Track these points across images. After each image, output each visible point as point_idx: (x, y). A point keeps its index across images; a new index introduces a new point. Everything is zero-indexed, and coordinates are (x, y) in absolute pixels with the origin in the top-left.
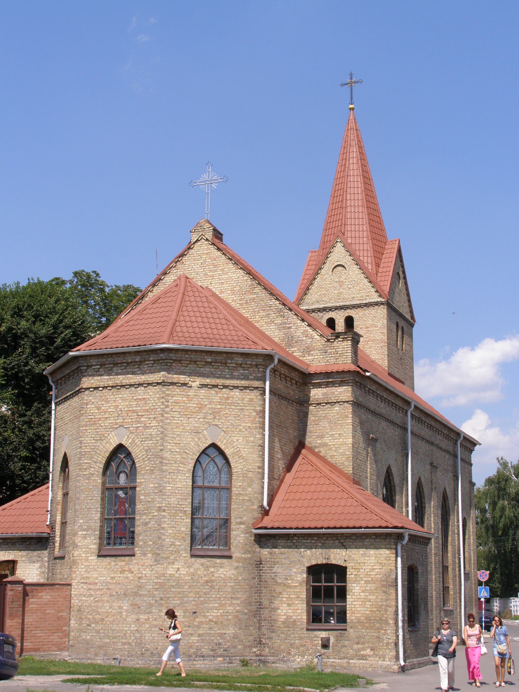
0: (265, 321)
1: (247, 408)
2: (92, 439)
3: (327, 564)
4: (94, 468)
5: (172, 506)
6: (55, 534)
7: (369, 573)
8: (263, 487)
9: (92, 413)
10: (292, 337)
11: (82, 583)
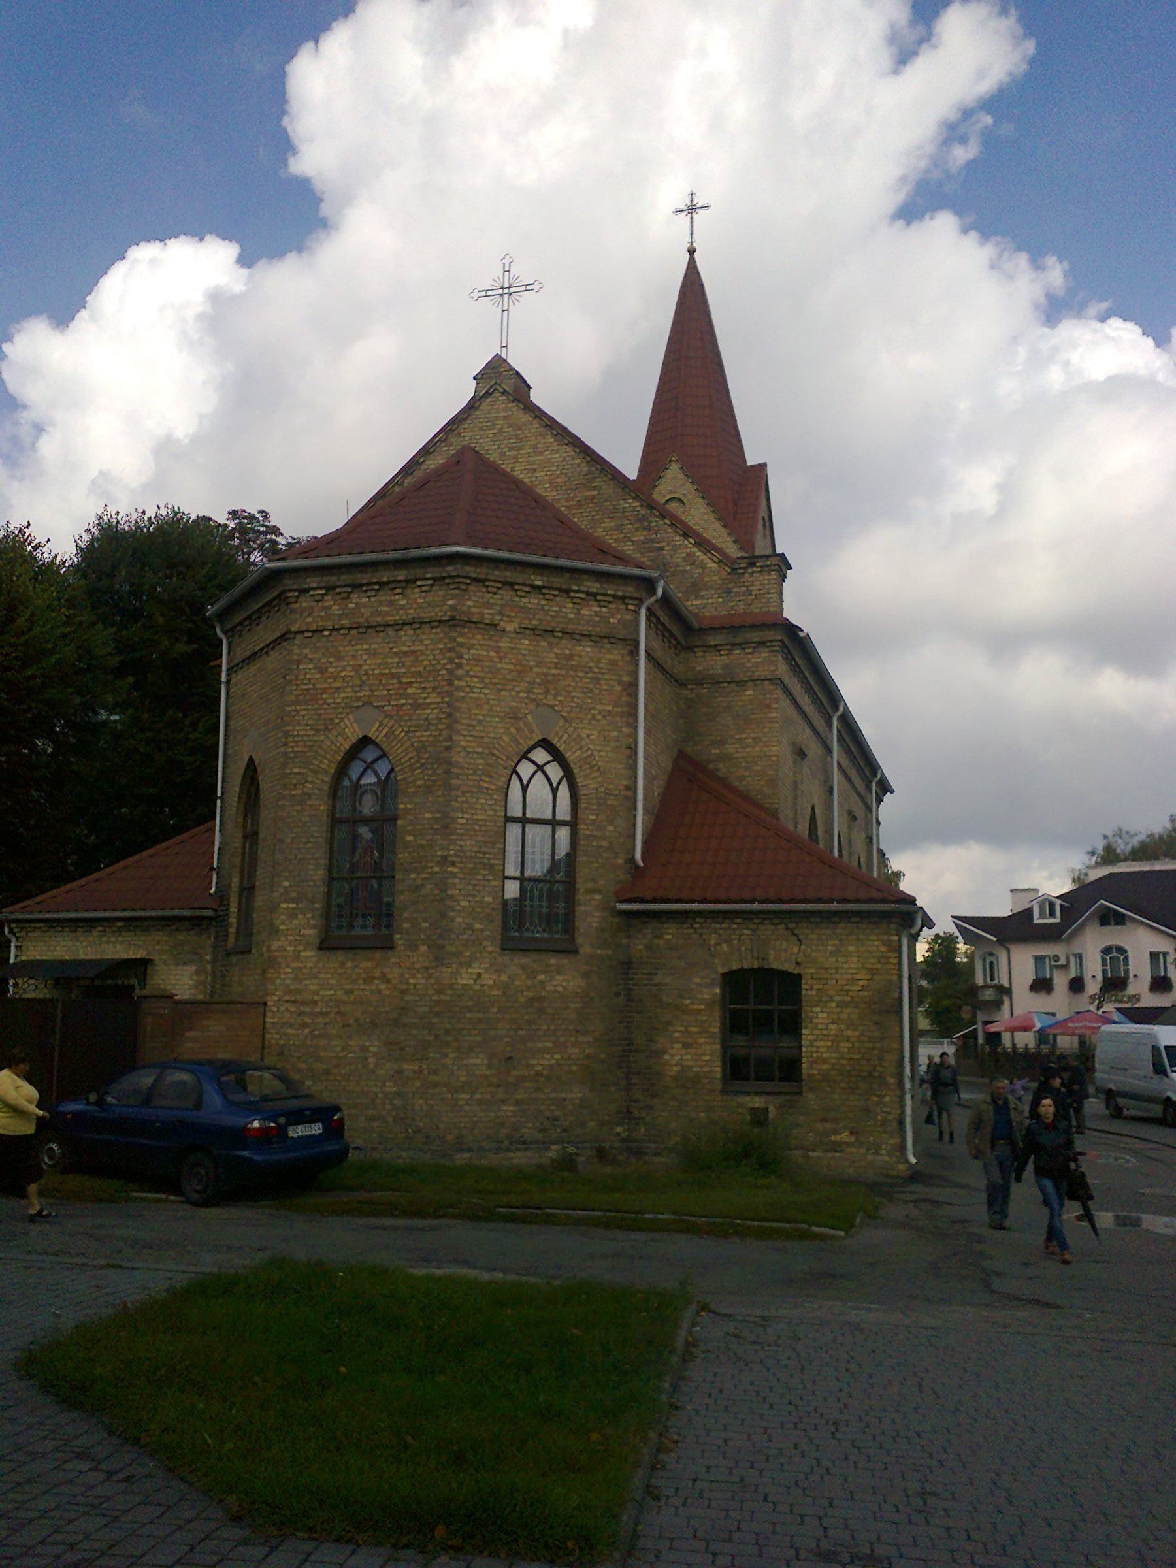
0: (614, 537)
1: (606, 676)
2: (308, 728)
4: (312, 782)
5: (468, 854)
6: (228, 910)
7: (847, 988)
8: (634, 825)
9: (310, 679)
10: (665, 565)
11: (287, 1001)
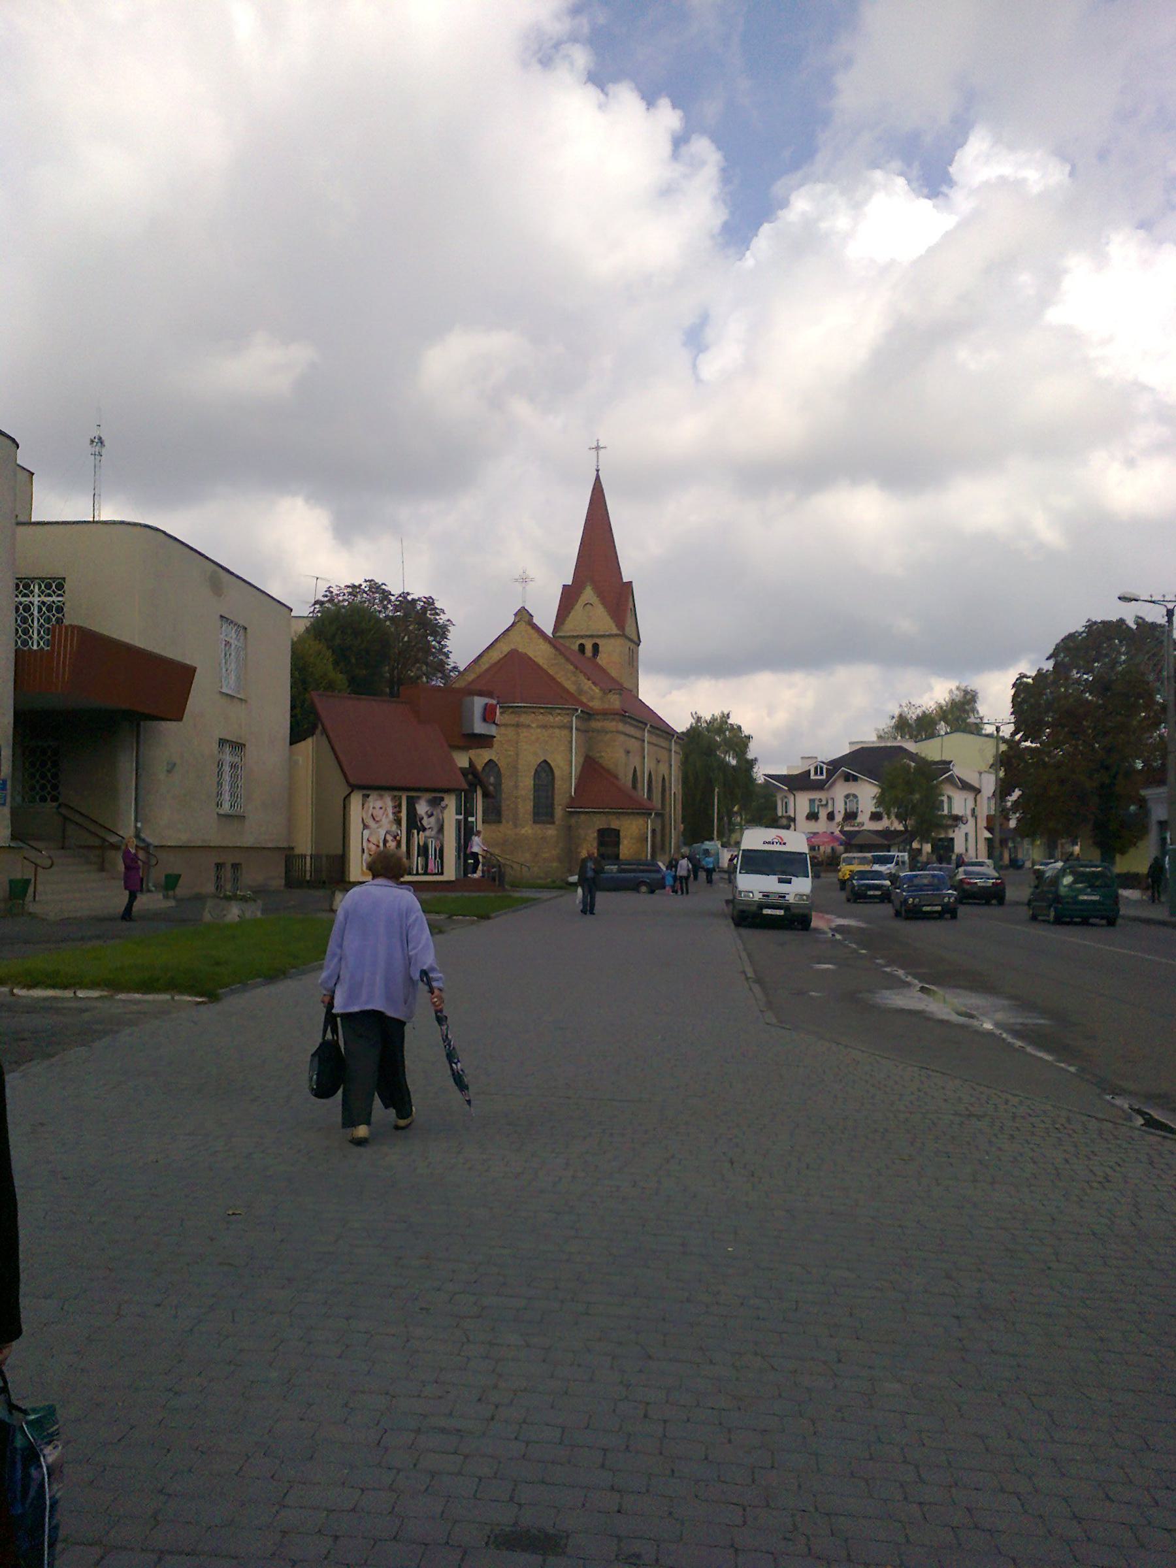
3: (608, 829)
